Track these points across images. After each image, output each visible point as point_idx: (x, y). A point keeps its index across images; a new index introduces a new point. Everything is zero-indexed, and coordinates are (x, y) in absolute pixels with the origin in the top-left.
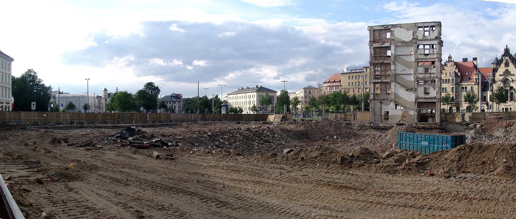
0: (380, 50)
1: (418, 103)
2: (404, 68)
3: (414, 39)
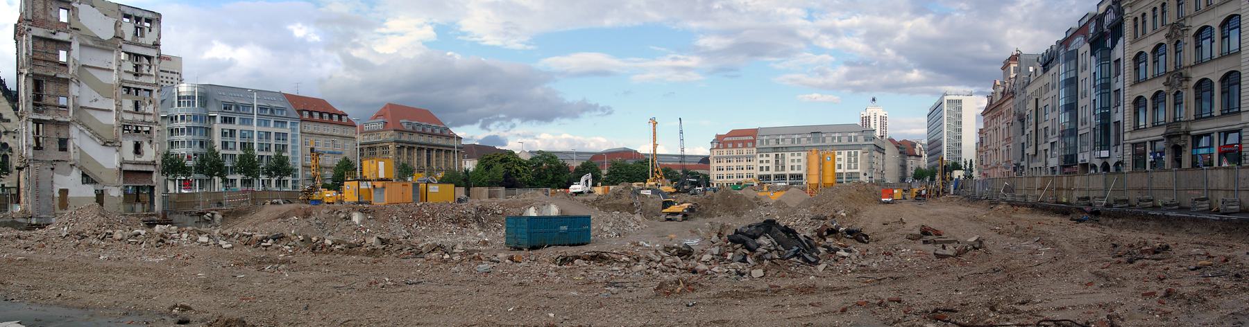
0: (45, 46)
1: (124, 171)
2: (97, 96)
3: (116, 37)
